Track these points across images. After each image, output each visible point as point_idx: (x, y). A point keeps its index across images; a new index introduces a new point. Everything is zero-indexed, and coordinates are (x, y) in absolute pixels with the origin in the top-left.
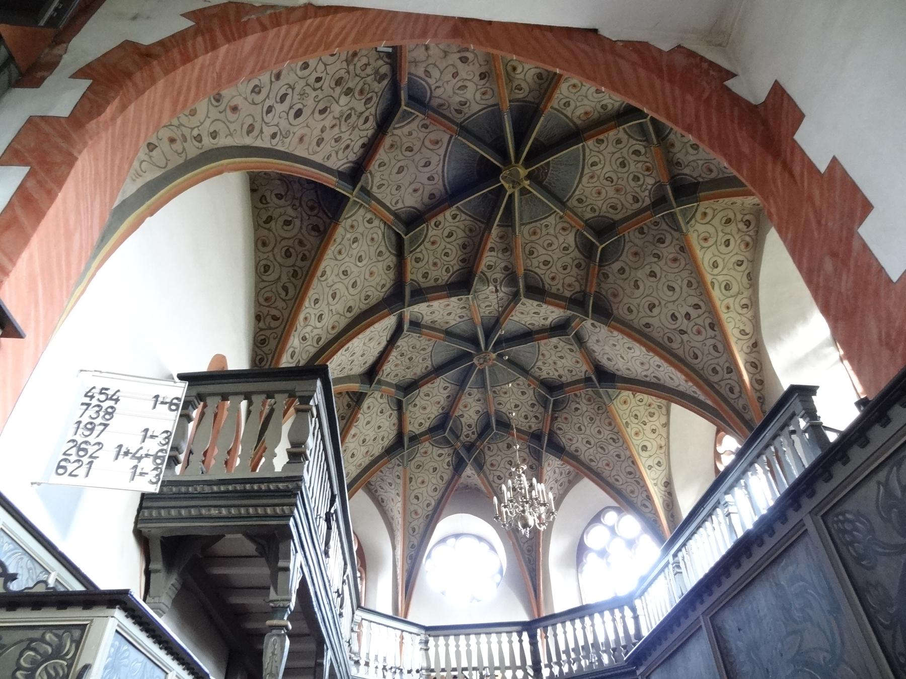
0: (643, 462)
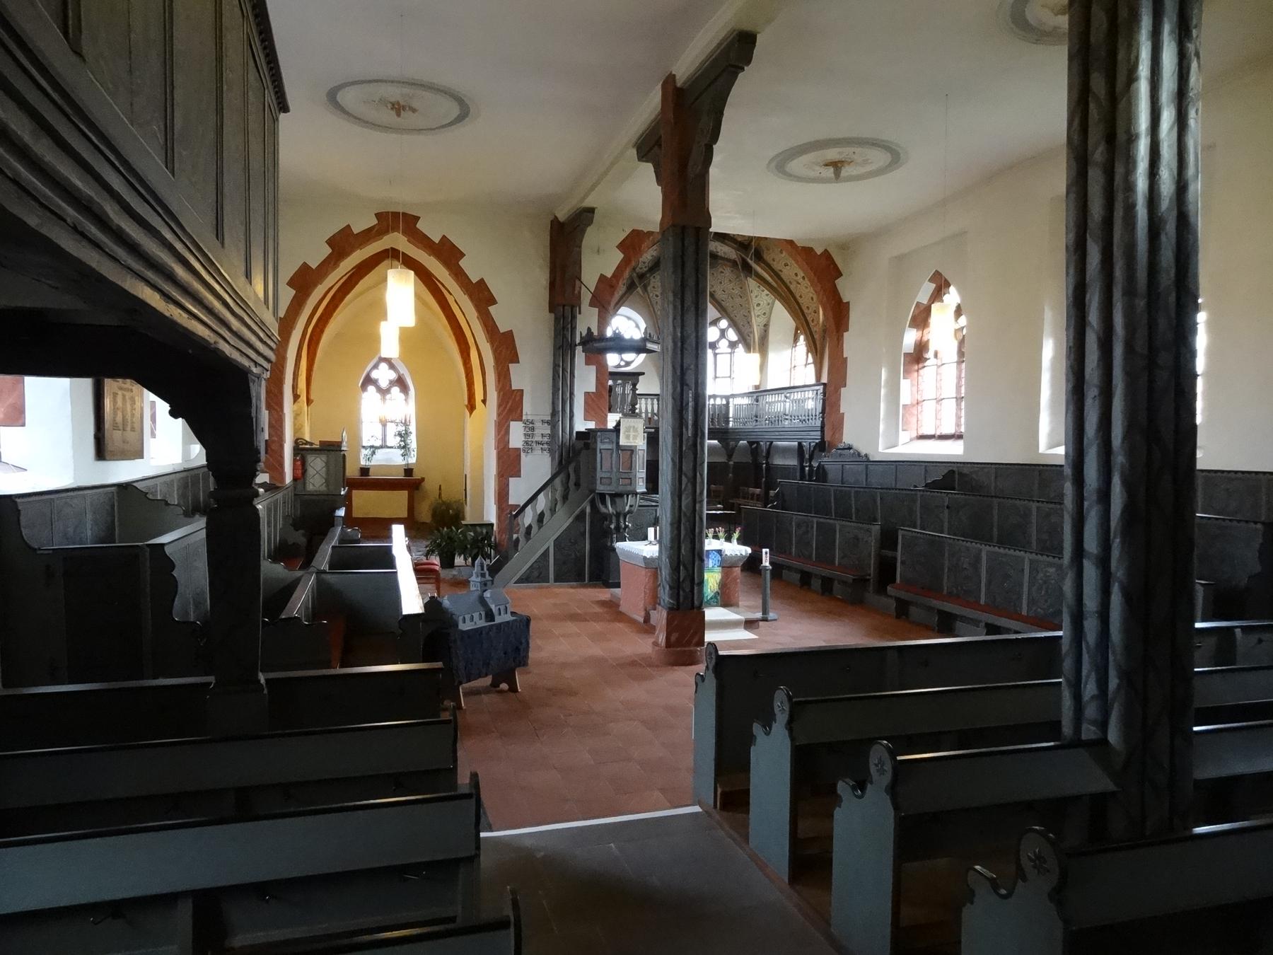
0: (756, 312)
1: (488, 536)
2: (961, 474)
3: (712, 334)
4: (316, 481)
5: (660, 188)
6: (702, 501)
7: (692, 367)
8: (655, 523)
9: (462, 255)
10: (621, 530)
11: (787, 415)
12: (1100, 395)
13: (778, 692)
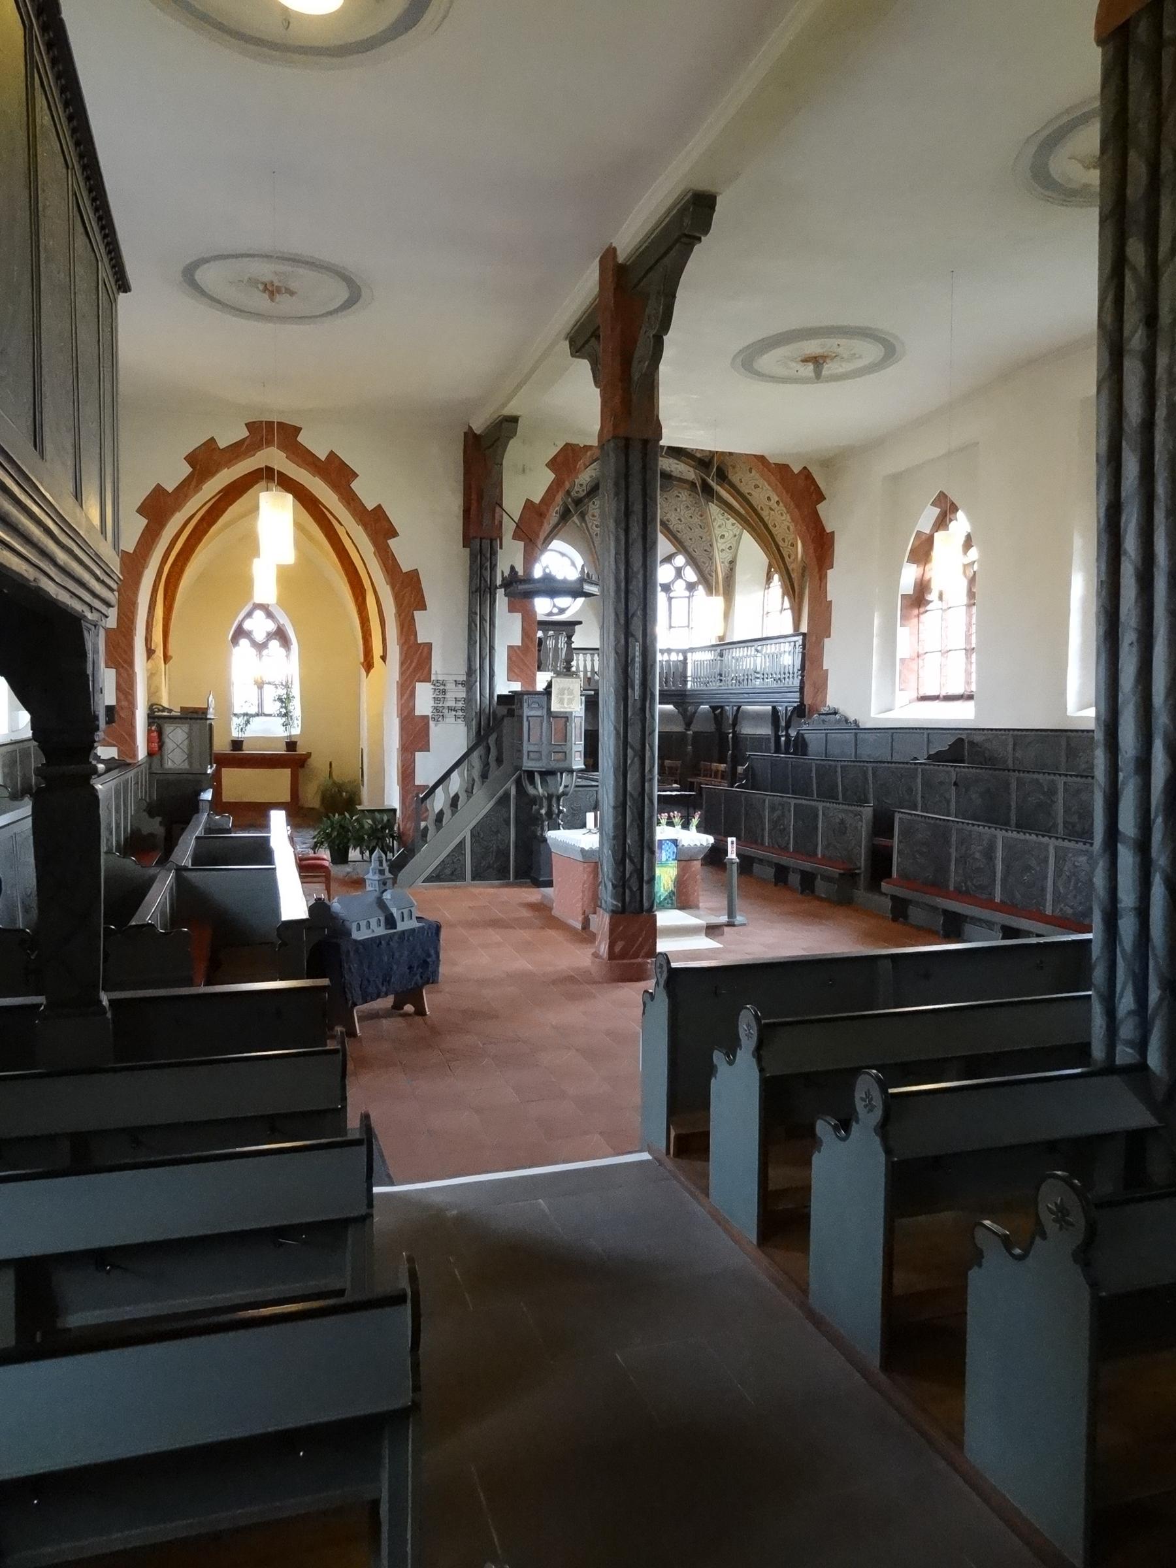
0: (720, 545)
1: (390, 824)
2: (971, 743)
3: (664, 573)
4: (176, 758)
5: (598, 390)
6: (651, 780)
7: (639, 613)
8: (595, 808)
9: (355, 475)
10: (554, 816)
11: (758, 673)
12: (1138, 640)
13: (743, 1012)
